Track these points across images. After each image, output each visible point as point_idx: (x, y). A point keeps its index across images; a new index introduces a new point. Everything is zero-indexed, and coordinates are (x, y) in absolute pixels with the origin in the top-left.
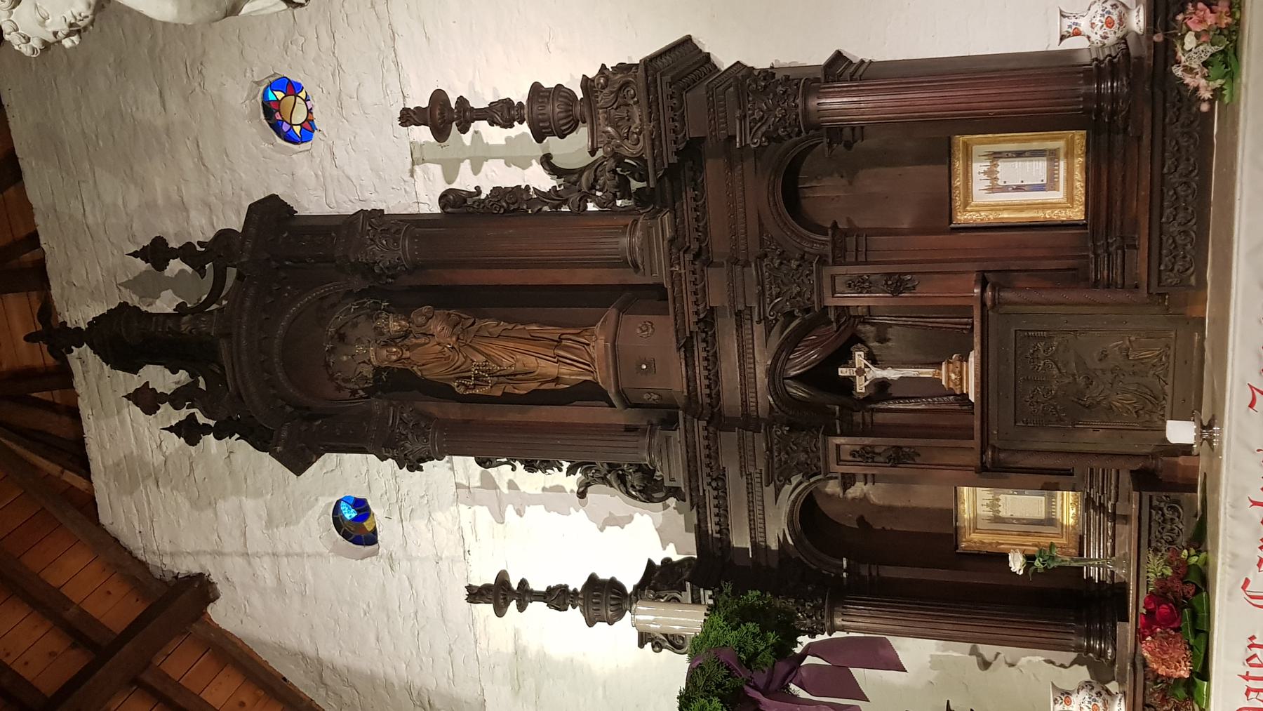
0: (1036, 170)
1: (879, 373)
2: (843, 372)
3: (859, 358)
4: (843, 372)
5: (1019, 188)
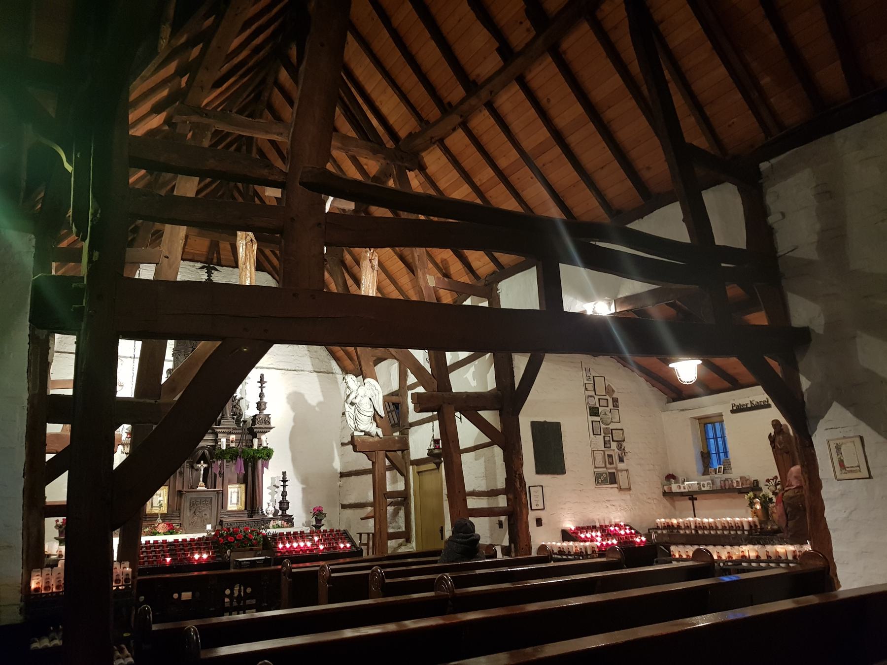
0: (234, 500)
1: (202, 470)
2: (202, 462)
3: (205, 465)
4: (202, 462)
5: (231, 497)
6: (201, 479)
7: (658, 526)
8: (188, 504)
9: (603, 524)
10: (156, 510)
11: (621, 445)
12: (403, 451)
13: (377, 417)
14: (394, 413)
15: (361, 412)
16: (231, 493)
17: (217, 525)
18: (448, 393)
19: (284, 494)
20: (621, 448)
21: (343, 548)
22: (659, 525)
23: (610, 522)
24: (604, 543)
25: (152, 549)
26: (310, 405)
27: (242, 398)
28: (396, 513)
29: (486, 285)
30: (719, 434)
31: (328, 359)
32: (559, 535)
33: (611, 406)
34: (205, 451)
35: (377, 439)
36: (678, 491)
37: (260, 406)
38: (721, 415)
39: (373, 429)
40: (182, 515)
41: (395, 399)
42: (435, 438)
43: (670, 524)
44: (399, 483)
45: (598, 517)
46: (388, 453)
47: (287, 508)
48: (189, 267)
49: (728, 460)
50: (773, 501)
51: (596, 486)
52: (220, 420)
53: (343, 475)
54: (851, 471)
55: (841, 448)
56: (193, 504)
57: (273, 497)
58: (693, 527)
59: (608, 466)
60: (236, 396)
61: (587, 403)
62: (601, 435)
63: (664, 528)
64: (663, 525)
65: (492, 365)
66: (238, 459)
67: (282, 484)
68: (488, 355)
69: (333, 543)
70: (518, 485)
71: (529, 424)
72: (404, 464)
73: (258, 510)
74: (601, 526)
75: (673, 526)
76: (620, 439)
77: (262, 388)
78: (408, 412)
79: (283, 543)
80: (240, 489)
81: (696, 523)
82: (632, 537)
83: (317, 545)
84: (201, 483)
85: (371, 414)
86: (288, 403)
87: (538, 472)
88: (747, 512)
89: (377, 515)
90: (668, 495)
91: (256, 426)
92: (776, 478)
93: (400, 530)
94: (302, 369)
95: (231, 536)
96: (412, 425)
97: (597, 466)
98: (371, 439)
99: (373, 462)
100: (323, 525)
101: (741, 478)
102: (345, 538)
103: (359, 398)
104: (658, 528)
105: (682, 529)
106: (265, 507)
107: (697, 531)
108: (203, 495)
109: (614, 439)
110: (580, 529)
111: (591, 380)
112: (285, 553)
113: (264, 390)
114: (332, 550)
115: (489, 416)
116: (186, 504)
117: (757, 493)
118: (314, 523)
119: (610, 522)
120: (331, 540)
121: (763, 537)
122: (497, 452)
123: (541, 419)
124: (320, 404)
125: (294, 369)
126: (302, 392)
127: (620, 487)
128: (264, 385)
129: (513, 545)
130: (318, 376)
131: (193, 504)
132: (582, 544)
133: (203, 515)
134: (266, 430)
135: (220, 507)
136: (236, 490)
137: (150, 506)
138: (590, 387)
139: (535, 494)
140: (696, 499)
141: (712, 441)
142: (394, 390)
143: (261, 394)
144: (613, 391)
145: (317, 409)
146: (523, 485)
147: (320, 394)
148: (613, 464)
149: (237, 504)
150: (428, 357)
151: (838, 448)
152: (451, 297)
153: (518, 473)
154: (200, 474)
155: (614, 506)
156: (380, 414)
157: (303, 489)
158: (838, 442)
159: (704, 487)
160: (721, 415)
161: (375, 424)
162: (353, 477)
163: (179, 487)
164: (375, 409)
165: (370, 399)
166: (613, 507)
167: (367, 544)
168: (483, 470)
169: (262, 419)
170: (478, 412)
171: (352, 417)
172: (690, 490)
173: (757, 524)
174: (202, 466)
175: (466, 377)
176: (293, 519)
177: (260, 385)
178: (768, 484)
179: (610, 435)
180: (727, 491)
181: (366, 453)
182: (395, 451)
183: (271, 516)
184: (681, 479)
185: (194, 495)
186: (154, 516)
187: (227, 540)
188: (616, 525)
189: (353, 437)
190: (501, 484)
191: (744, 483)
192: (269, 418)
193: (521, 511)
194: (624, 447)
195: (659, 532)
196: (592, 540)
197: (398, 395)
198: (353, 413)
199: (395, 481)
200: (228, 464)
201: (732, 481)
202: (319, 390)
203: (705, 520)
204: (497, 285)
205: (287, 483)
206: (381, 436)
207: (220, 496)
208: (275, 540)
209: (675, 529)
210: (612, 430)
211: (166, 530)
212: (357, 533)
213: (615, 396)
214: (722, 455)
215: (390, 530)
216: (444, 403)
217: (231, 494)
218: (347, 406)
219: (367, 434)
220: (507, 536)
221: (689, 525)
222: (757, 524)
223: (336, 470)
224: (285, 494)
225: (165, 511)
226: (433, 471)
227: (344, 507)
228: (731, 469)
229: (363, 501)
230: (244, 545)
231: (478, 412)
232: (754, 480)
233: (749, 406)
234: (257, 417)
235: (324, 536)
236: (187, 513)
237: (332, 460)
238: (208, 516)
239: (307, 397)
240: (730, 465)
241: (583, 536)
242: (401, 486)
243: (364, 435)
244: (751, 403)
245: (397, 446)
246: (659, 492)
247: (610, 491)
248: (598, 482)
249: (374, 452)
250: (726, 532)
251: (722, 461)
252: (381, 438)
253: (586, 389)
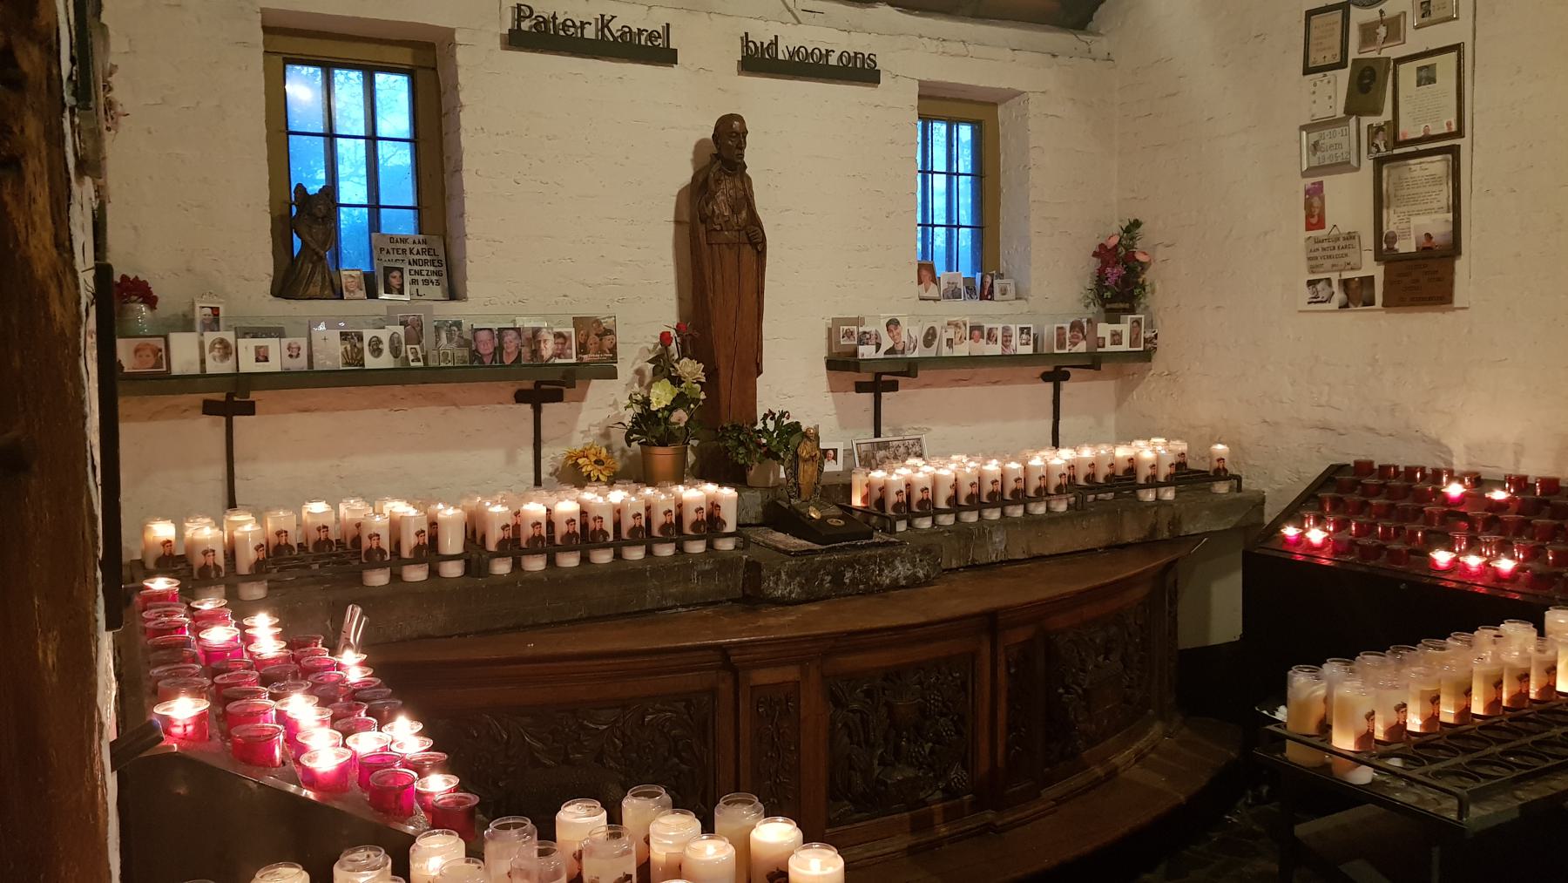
36: (214, 366)
88: (511, 459)
101: (578, 322)
140: (249, 409)
159: (376, 351)
191: (592, 347)
233: (590, 33)
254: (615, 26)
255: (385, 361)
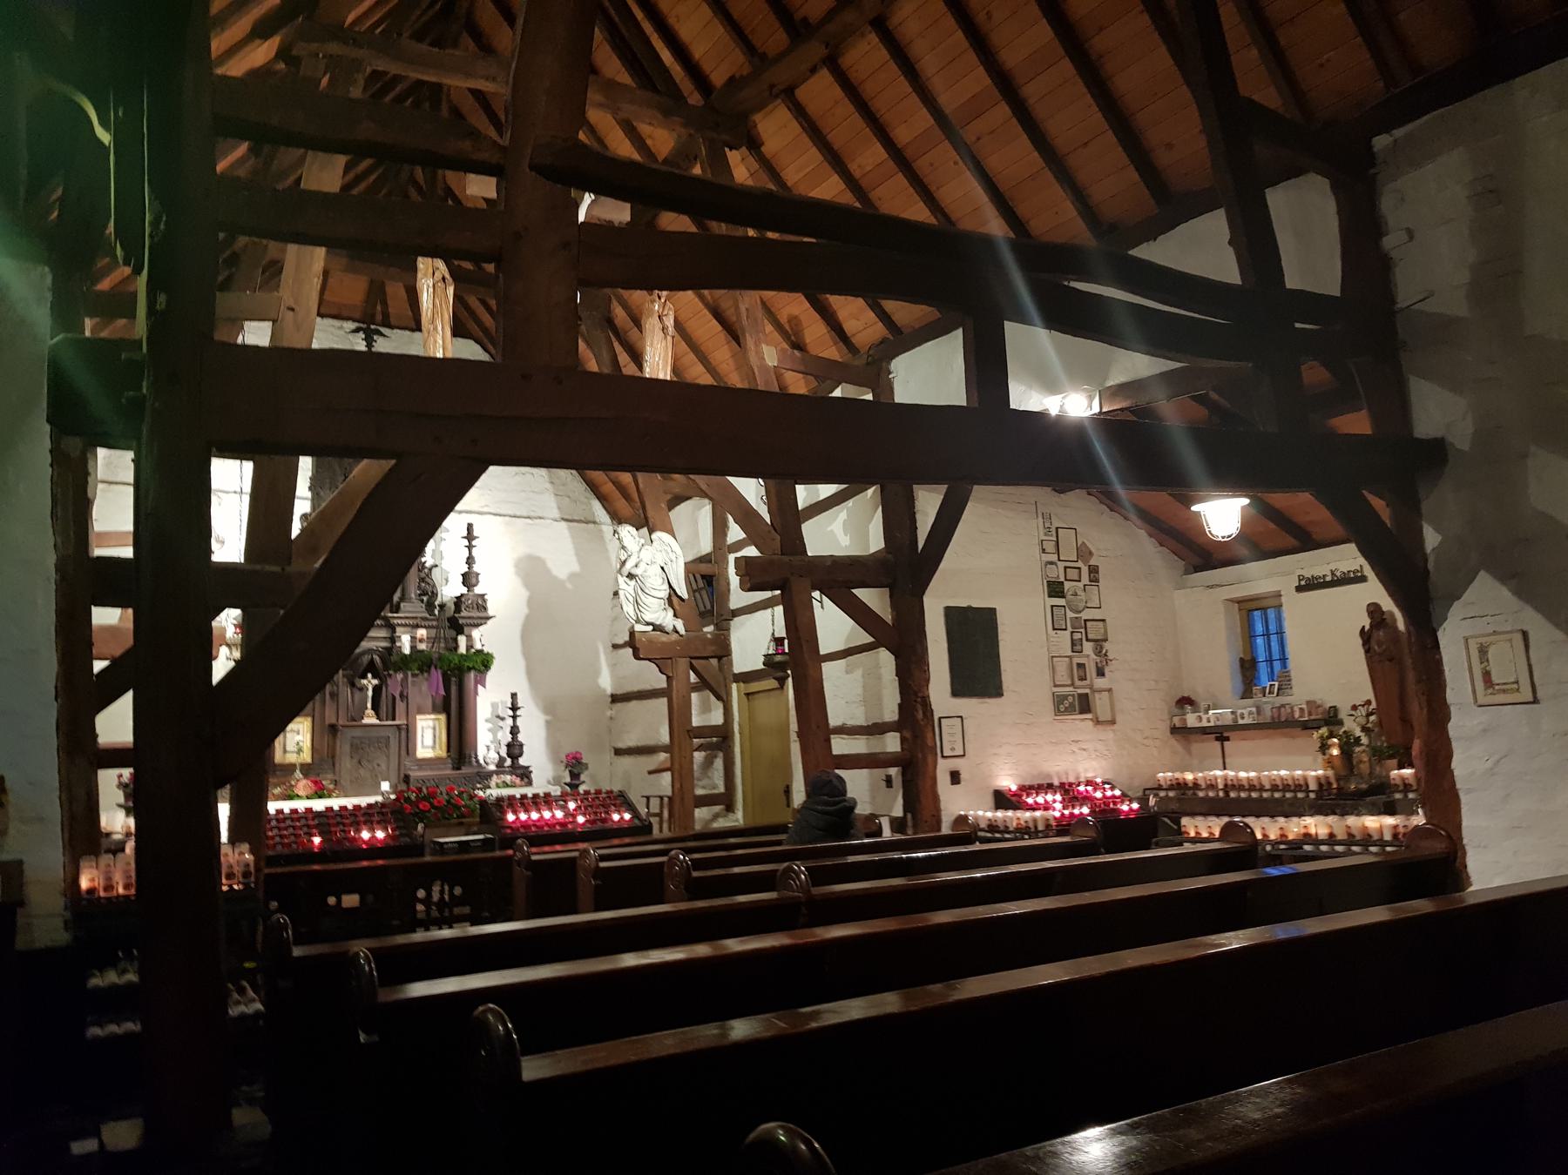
0: (429, 741)
2: (369, 675)
3: (375, 682)
4: (369, 675)
5: (422, 736)
6: (369, 705)
7: (1160, 785)
8: (347, 748)
9: (1064, 780)
10: (292, 758)
11: (1102, 647)
12: (720, 658)
13: (675, 600)
14: (704, 593)
15: (647, 591)
16: (423, 728)
17: (399, 782)
18: (799, 558)
19: (514, 731)
20: (1100, 652)
21: (619, 821)
22: (1162, 783)
23: (1078, 778)
24: (1066, 812)
25: (289, 822)
26: (555, 578)
27: (436, 566)
28: (708, 763)
29: (868, 364)
30: (1273, 628)
31: (586, 498)
32: (990, 800)
33: (1085, 579)
34: (374, 656)
35: (674, 637)
37: (469, 579)
38: (1278, 595)
39: (668, 619)
40: (337, 765)
41: (705, 568)
42: (777, 635)
43: (1181, 781)
44: (713, 713)
45: (1057, 768)
46: (693, 661)
47: (521, 755)
48: (332, 329)
49: (1287, 672)
50: (1362, 742)
51: (1056, 718)
52: (399, 604)
53: (616, 699)
54: (1504, 691)
55: (1487, 652)
56: (356, 748)
57: (495, 736)
58: (1221, 786)
59: (1078, 683)
60: (425, 562)
61: (1044, 575)
62: (1066, 630)
63: (1171, 788)
64: (1169, 783)
65: (878, 507)
66: (433, 669)
67: (511, 713)
68: (870, 491)
69: (601, 813)
70: (920, 715)
71: (942, 612)
72: (722, 679)
73: (470, 757)
74: (1062, 785)
75: (1186, 784)
76: (1099, 638)
77: (470, 547)
78: (729, 590)
79: (515, 812)
80: (437, 722)
81: (1226, 779)
82: (1115, 803)
83: (574, 816)
84: (369, 711)
85: (664, 593)
86: (517, 574)
87: (956, 693)
88: (1315, 760)
89: (677, 766)
90: (1180, 732)
91: (462, 614)
92: (1368, 702)
93: (716, 791)
94: (541, 515)
95: (425, 800)
96: (736, 613)
97: (1058, 683)
98: (664, 638)
99: (668, 677)
100: (584, 782)
101: (1308, 703)
102: (621, 805)
103: (642, 566)
104: (1160, 788)
105: (1202, 790)
106: (481, 752)
107: (1227, 793)
108: (374, 733)
109: (1090, 636)
110: (1026, 789)
111: (1052, 535)
112: (518, 829)
113: (474, 551)
114: (599, 824)
115: (872, 597)
116: (343, 747)
117: (1334, 728)
118: (568, 780)
119: (1078, 778)
120: (597, 807)
121: (1342, 802)
122: (885, 659)
123: (962, 603)
124: (573, 576)
125: (525, 514)
126: (542, 555)
127: (1097, 718)
128: (474, 543)
129: (909, 816)
130: (569, 528)
131: (359, 749)
132: (1028, 814)
133: (376, 767)
134: (479, 621)
135: (403, 752)
136: (431, 723)
137: (282, 749)
138: (1050, 547)
139: (950, 731)
140: (1228, 739)
141: (1260, 641)
142: (704, 553)
143: (468, 558)
144: (1091, 554)
145: (569, 586)
146: (929, 714)
147: (574, 559)
148: (1086, 679)
149: (434, 747)
150: (764, 493)
151: (1483, 651)
152: (806, 387)
153: (920, 695)
154: (367, 695)
155: (1084, 750)
156: (679, 594)
157: (548, 722)
158: (1483, 640)
159: (1243, 718)
160: (1278, 595)
161: (670, 613)
162: (634, 704)
163: (330, 718)
164: (670, 586)
165: (662, 568)
166: (1084, 752)
167: (660, 815)
168: (860, 691)
169: (472, 604)
170: (853, 590)
171: (631, 599)
172: (1219, 723)
173: (1333, 780)
174: (370, 682)
175: (832, 531)
176: (531, 772)
177: (468, 544)
178: (1353, 713)
179: (1083, 630)
180: (1281, 724)
181: (656, 661)
182: (706, 658)
183: (492, 767)
184: (1203, 705)
185: (358, 733)
186: (290, 768)
187: (418, 808)
188: (1088, 783)
189: (632, 633)
190: (890, 713)
192: (485, 601)
193: (925, 758)
194: (1106, 652)
195: (1162, 794)
196: (1047, 807)
197: (711, 562)
198: (632, 592)
199: (706, 709)
200: (415, 679)
201: (1292, 708)
202: (572, 552)
203: (1243, 774)
204: (889, 363)
205: (518, 713)
206: (682, 630)
207: (403, 734)
208: (502, 807)
209: (1190, 788)
210: (1085, 621)
211: (310, 792)
212: (643, 797)
213: (1092, 562)
214: (1277, 665)
215: (699, 792)
216: (792, 574)
217: (423, 731)
218: (622, 580)
219: (657, 628)
220: (900, 801)
221: (1214, 783)
222: (1333, 780)
223: (604, 691)
224: (516, 730)
225: (309, 760)
226: (772, 693)
227: (619, 752)
228: (1291, 688)
229: (651, 742)
230: (447, 816)
231: (853, 590)
232: (1331, 707)
233: (1328, 579)
234: (463, 599)
235: (585, 801)
236: (346, 763)
237: (597, 673)
238: (384, 767)
239: (550, 564)
240: (1290, 680)
241: (1030, 801)
242: (717, 718)
243: (654, 630)
244: (1333, 573)
245: (710, 650)
246: (1164, 727)
247: (1080, 725)
248: (1059, 710)
249: (670, 661)
250: (1277, 795)
251: (1276, 673)
252: (681, 636)
253: (1044, 551)
254: (1338, 574)
255: (1247, 721)
